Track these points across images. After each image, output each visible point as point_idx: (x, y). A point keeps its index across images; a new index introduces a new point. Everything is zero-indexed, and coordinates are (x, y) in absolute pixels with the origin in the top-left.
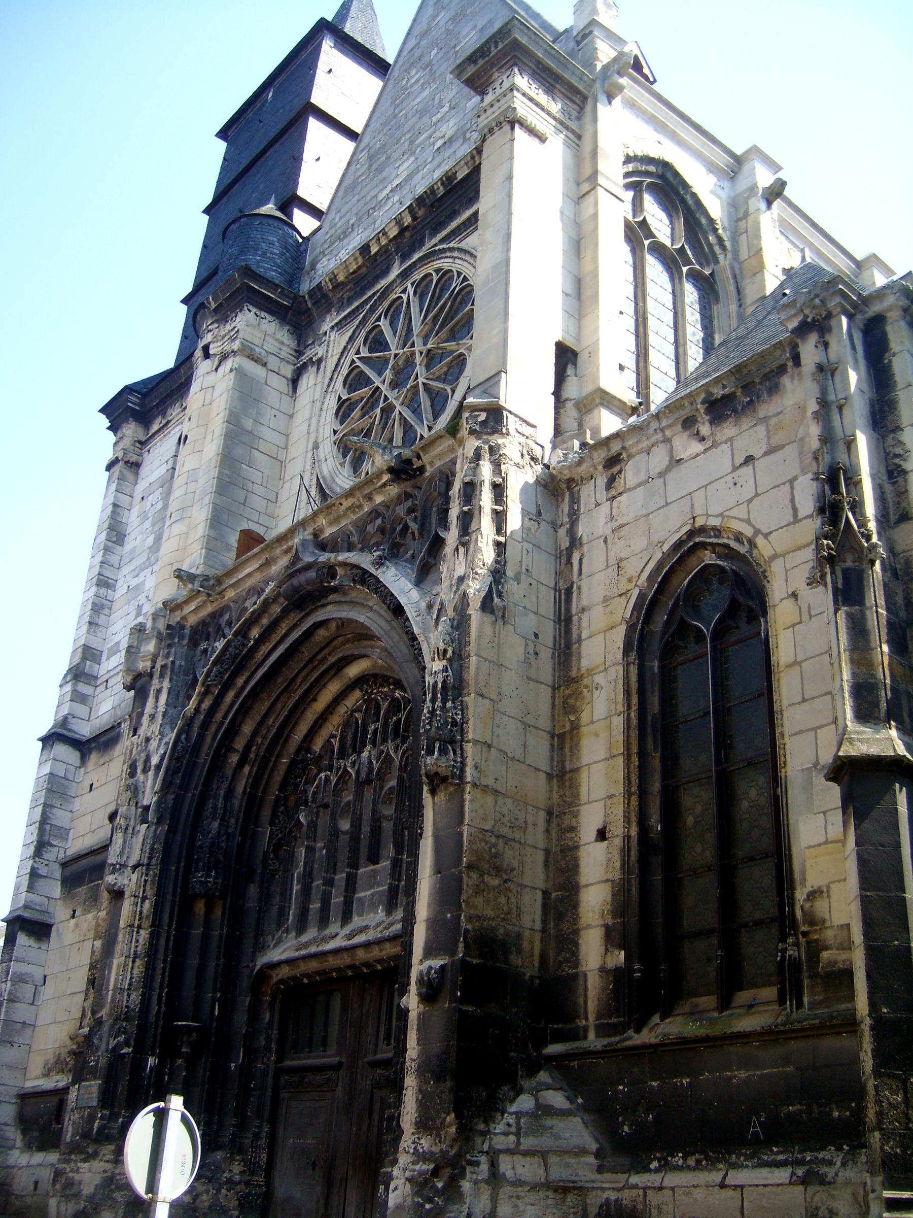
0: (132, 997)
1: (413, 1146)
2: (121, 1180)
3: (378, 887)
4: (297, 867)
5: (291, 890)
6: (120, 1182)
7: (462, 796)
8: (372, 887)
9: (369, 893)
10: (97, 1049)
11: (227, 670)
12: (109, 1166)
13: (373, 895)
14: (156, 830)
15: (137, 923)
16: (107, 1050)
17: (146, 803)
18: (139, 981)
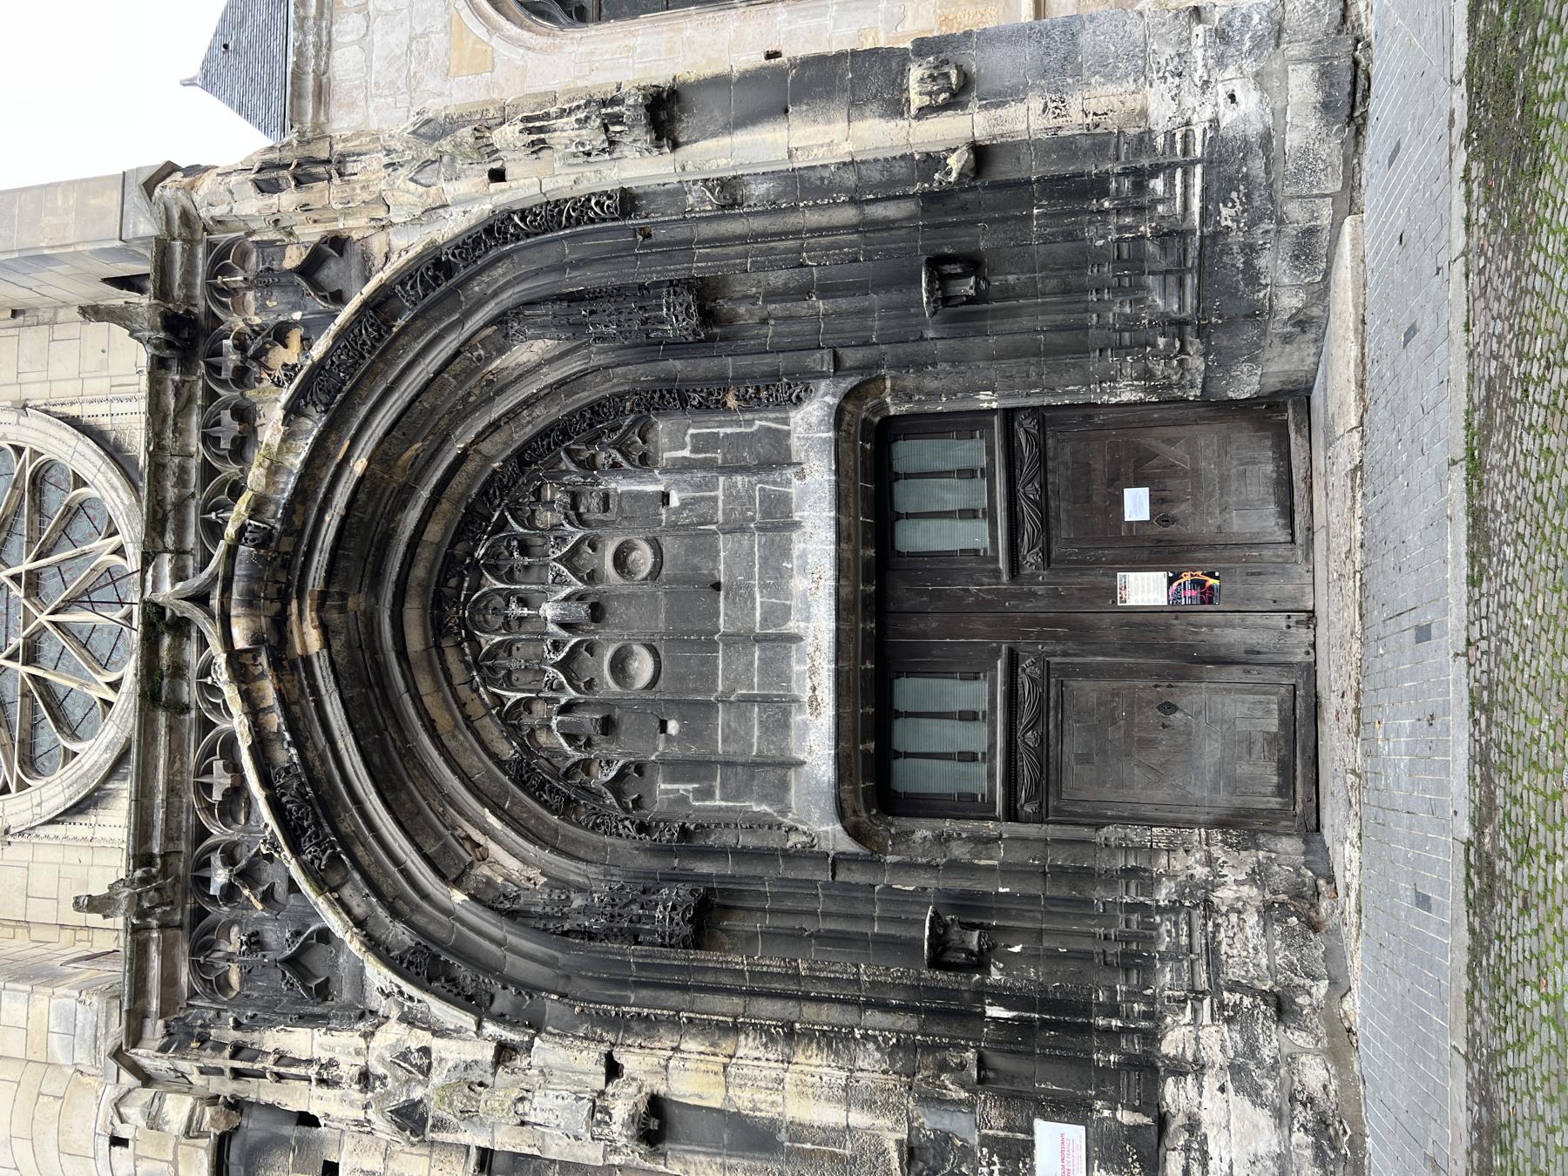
0: (866, 1066)
1: (1170, 79)
2: (1235, 1047)
3: (752, 578)
4: (683, 800)
5: (720, 809)
6: (1240, 1045)
7: (691, 85)
8: (750, 589)
9: (758, 596)
10: (966, 1153)
11: (318, 824)
12: (1210, 1082)
13: (763, 586)
14: (550, 1034)
15: (721, 1059)
16: (971, 1106)
17: (488, 1053)
18: (837, 1053)
